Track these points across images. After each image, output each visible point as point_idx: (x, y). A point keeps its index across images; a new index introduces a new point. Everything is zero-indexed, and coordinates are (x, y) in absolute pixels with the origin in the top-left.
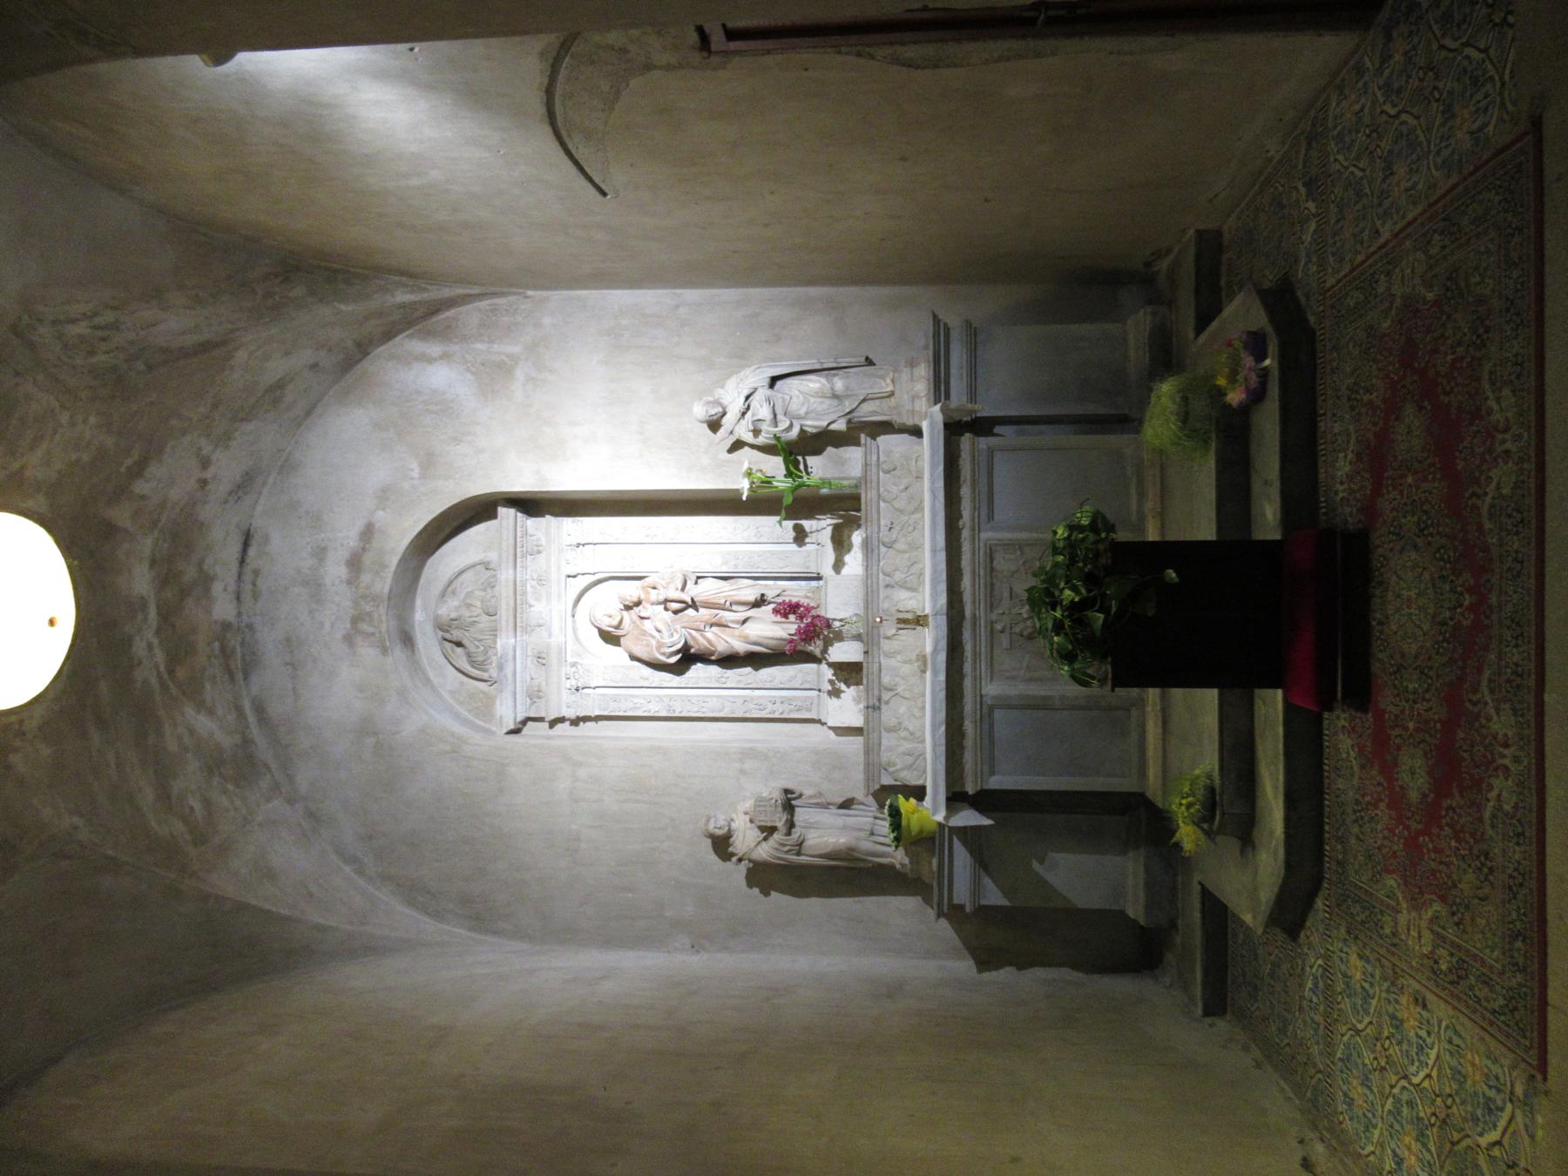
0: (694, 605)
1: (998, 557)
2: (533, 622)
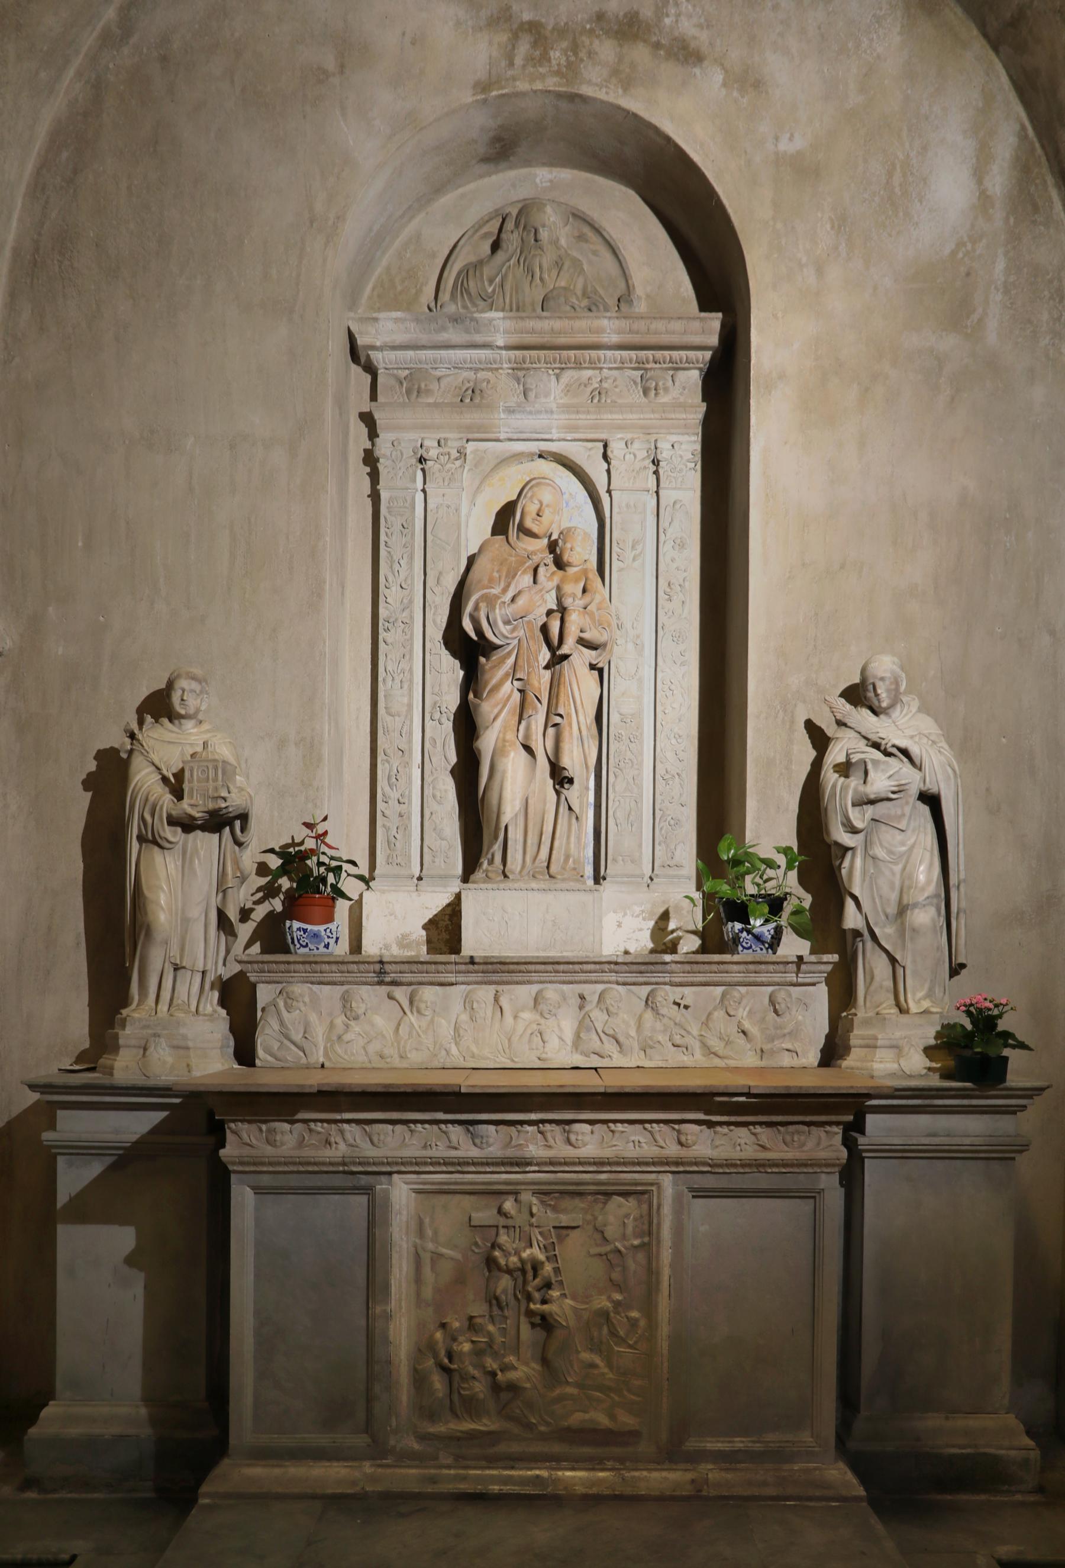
1: (631, 1204)
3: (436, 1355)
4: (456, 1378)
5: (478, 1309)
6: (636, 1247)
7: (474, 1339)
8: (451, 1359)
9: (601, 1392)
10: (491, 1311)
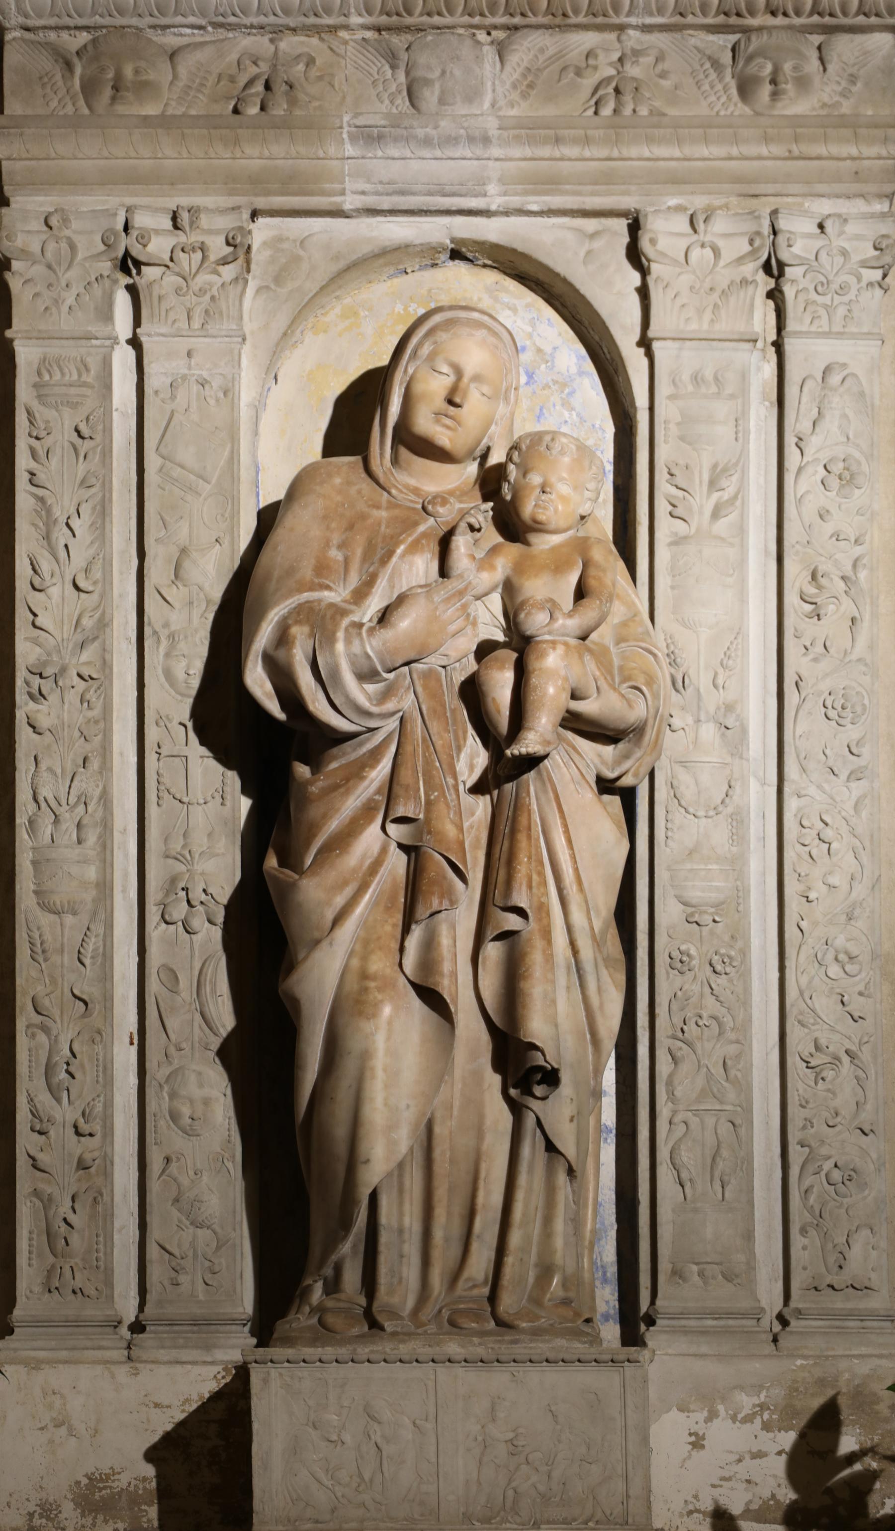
0: (507, 770)
2: (428, 61)
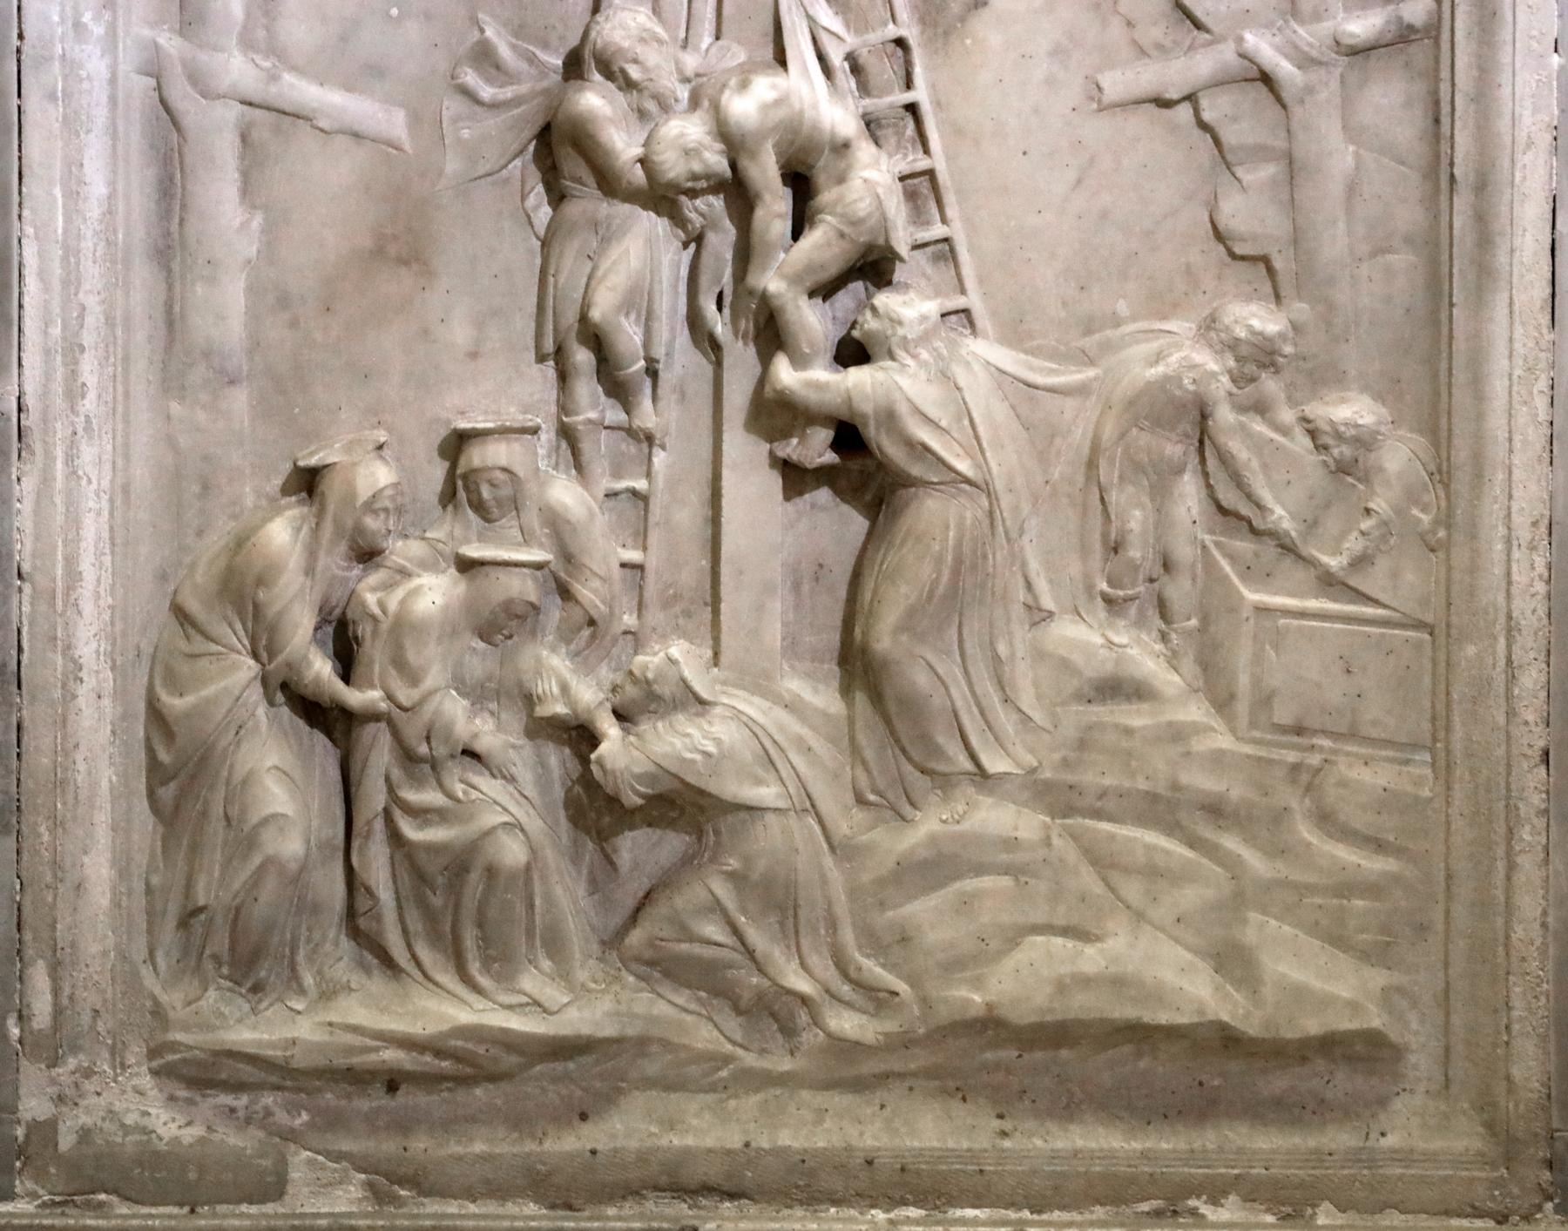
3: (263, 639)
4: (379, 756)
5: (503, 393)
6: (1358, 52)
7: (473, 551)
8: (346, 658)
9: (1172, 828)
10: (565, 406)
